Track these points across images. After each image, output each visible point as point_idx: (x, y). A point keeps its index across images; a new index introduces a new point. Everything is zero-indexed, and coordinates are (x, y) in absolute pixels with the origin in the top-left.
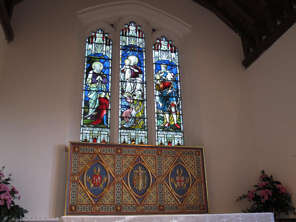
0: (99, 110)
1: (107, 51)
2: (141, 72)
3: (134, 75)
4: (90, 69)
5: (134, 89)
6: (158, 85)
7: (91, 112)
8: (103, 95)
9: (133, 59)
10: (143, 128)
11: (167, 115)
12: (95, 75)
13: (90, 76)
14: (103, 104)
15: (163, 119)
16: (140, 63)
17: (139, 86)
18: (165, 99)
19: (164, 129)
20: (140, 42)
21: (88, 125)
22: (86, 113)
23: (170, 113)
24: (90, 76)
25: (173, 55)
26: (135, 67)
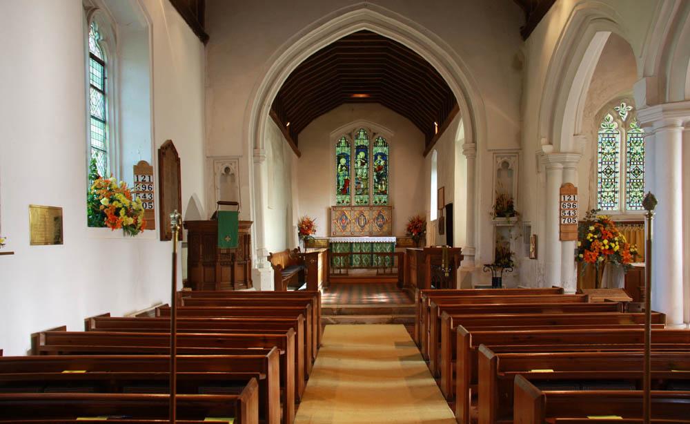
0: (345, 186)
1: (346, 150)
2: (366, 162)
3: (363, 164)
4: (339, 163)
5: (362, 172)
6: (375, 169)
7: (341, 187)
8: (346, 177)
9: (362, 154)
10: (367, 194)
11: (380, 186)
12: (342, 166)
13: (339, 167)
14: (347, 182)
15: (377, 188)
16: (366, 157)
17: (365, 171)
18: (379, 177)
19: (378, 194)
20: (365, 142)
21: (339, 193)
22: (338, 188)
23: (381, 185)
24: (339, 167)
25: (385, 148)
26: (363, 159)
